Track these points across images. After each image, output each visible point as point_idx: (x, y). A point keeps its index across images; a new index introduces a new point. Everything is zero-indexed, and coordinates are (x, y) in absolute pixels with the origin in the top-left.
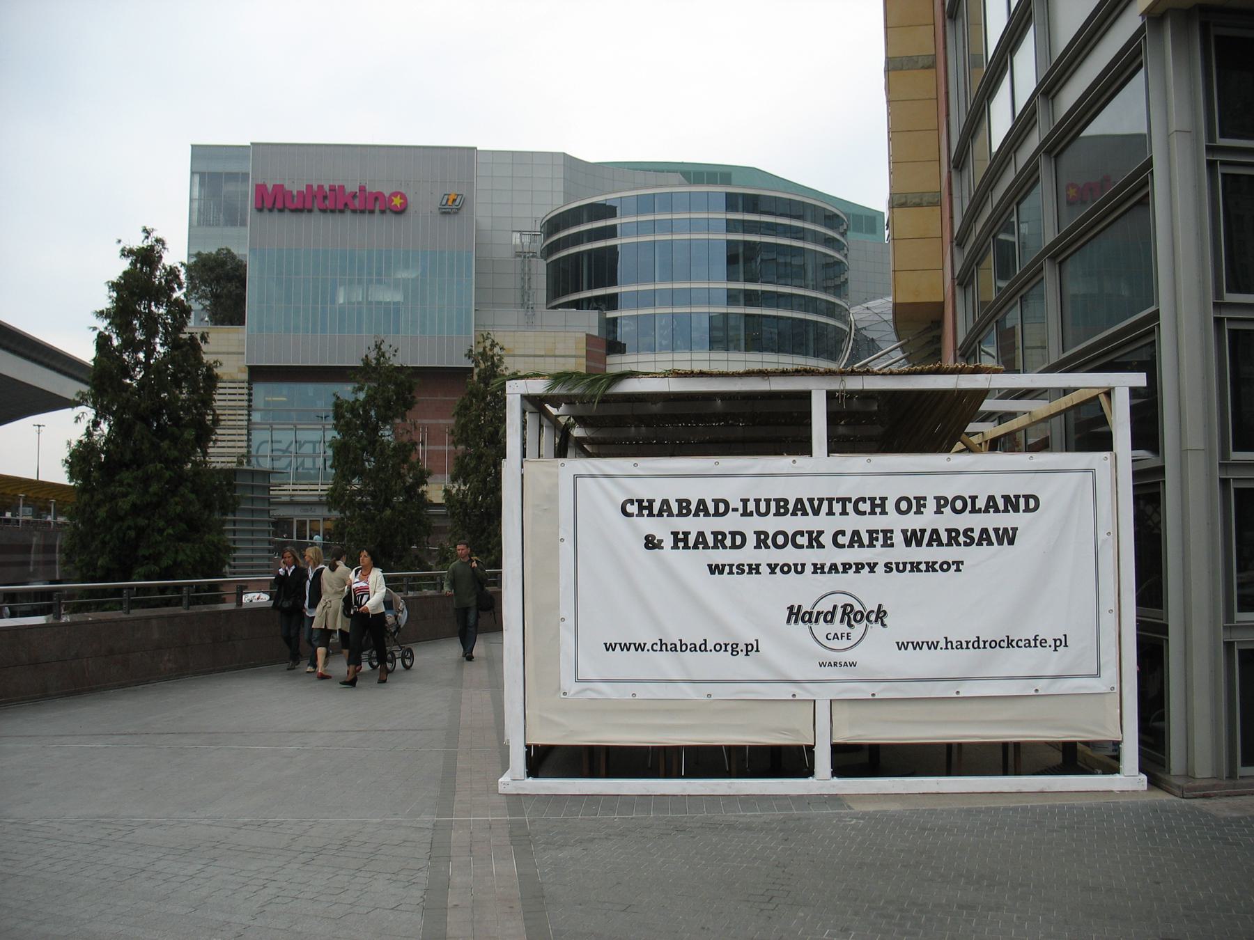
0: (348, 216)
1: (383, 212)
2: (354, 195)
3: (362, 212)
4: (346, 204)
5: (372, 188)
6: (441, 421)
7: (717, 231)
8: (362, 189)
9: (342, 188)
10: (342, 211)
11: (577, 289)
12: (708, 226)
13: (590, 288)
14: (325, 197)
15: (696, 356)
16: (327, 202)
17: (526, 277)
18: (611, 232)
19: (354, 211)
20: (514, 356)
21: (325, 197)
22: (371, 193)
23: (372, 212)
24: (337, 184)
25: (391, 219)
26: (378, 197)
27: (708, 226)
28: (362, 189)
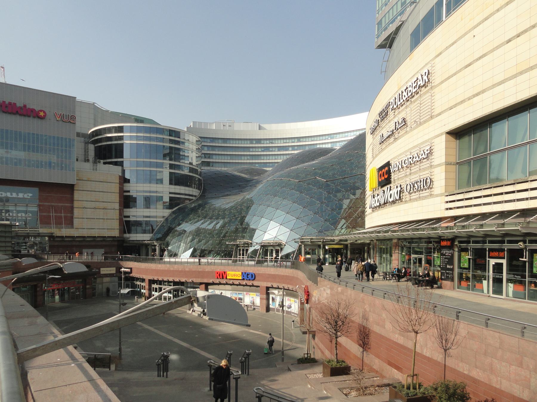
0: (18, 117)
1: (34, 117)
2: (20, 108)
3: (24, 116)
4: (17, 112)
5: (31, 106)
6: (59, 204)
7: (166, 143)
8: (25, 106)
9: (15, 104)
10: (14, 114)
11: (111, 158)
12: (163, 140)
13: (116, 157)
14: (6, 107)
15: (151, 185)
16: (7, 109)
17: (86, 151)
18: (121, 138)
19: (21, 115)
20: (83, 180)
21: (6, 107)
22: (29, 109)
23: (29, 116)
24: (13, 102)
25: (36, 121)
26: (33, 110)
27: (163, 140)
28: (25, 106)
